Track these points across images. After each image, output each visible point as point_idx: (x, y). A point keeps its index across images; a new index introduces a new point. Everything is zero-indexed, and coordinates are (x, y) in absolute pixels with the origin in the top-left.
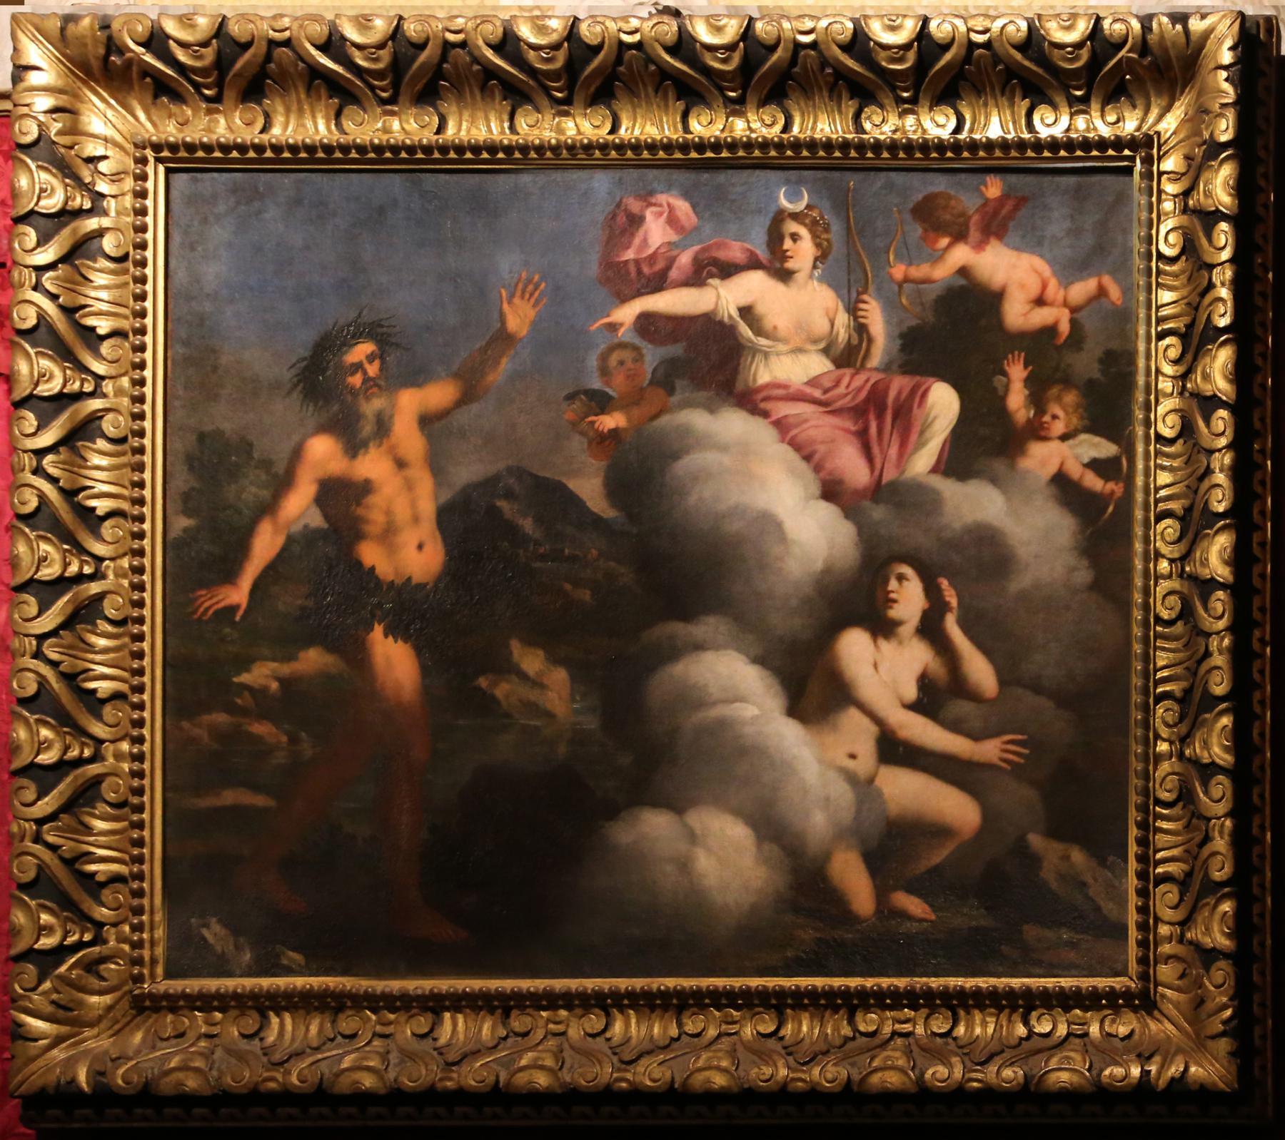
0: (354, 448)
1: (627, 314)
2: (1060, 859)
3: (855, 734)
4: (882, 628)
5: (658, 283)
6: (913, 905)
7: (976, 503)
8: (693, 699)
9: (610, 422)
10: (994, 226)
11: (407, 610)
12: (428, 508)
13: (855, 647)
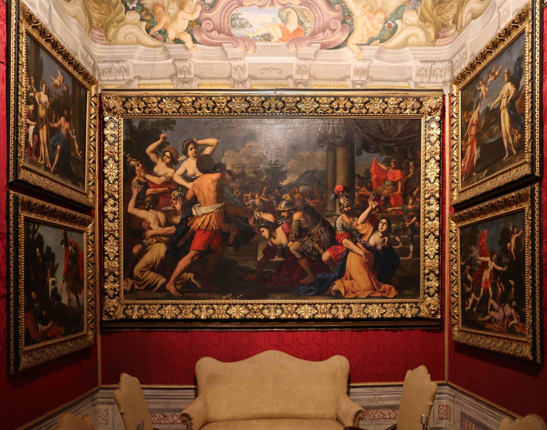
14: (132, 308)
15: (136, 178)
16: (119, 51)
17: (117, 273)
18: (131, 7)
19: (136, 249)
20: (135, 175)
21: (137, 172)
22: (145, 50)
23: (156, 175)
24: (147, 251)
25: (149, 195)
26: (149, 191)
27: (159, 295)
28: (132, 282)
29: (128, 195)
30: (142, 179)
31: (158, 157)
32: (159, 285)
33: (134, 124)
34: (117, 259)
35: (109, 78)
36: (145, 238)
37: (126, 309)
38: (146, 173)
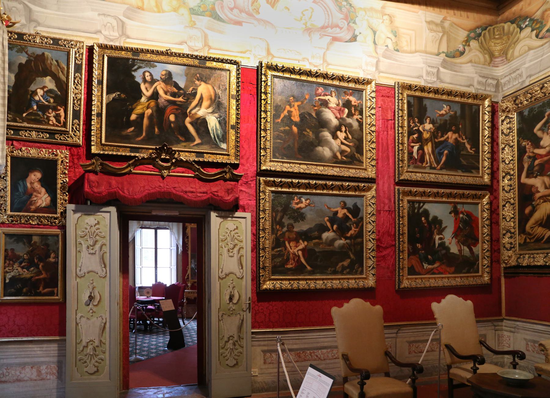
0: (291, 108)
1: (317, 98)
2: (357, 155)
3: (338, 141)
4: (341, 131)
5: (320, 96)
6: (344, 158)
7: (349, 120)
8: (324, 136)
9: (316, 108)
10: (351, 95)
11: (296, 124)
12: (298, 114)
13: (339, 133)
14: (524, 257)
15: (527, 154)
16: (514, 64)
17: (513, 230)
18: (524, 26)
19: (527, 211)
20: (526, 152)
21: (527, 150)
22: (535, 52)
23: (542, 147)
24: (536, 211)
25: (537, 165)
26: (537, 162)
27: (546, 246)
28: (525, 236)
29: (520, 169)
30: (531, 154)
31: (543, 133)
32: (546, 237)
33: (525, 114)
34: (512, 220)
35: (509, 87)
36: (534, 200)
37: (519, 258)
38: (534, 148)
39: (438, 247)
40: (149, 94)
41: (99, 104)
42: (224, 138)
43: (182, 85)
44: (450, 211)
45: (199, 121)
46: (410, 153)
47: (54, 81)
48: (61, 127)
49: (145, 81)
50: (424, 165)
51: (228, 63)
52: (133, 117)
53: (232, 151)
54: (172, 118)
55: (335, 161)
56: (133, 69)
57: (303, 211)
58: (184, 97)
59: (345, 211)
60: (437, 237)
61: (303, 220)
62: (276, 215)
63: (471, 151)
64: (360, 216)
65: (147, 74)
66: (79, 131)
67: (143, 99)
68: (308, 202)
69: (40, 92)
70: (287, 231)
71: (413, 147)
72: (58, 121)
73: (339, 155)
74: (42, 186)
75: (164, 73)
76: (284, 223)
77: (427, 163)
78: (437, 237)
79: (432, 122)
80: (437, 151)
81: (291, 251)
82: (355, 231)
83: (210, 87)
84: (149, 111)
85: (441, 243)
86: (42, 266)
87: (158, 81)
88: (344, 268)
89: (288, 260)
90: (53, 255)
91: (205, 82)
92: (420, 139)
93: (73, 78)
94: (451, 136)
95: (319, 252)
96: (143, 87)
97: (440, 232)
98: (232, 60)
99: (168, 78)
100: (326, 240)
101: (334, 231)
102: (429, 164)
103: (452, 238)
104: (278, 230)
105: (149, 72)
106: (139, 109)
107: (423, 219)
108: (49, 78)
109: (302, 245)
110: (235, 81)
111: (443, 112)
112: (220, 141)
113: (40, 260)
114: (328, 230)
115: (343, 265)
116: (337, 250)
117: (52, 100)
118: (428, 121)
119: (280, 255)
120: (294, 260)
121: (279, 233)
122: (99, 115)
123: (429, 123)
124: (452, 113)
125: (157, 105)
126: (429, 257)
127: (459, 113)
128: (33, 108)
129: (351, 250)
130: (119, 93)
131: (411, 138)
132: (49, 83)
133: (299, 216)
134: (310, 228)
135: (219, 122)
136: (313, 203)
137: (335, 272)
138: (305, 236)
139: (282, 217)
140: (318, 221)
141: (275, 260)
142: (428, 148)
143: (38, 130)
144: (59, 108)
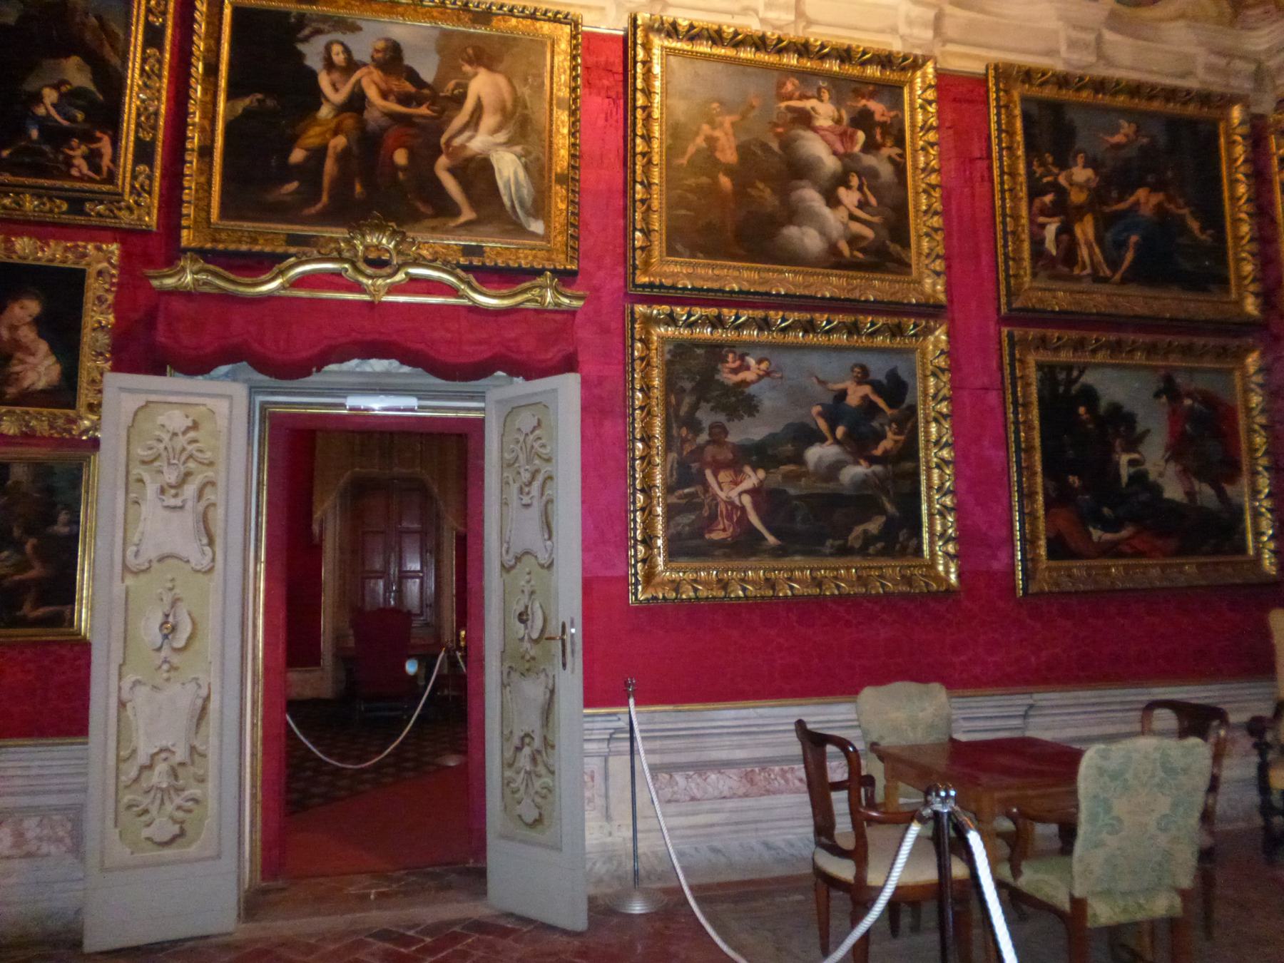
0: (714, 128)
1: (783, 105)
2: (895, 248)
3: (842, 213)
4: (849, 187)
5: (790, 98)
6: (860, 255)
7: (869, 160)
8: (802, 200)
9: (780, 130)
10: (872, 96)
11: (729, 171)
12: (733, 145)
13: (842, 192)
39: (1128, 485)
40: (338, 97)
41: (206, 123)
42: (540, 208)
43: (428, 75)
44: (1154, 389)
45: (473, 165)
46: (1037, 243)
47: (88, 68)
48: (104, 182)
49: (330, 65)
50: (1076, 271)
51: (549, 20)
52: (297, 155)
53: (559, 238)
54: (401, 157)
55: (833, 260)
56: (301, 35)
57: (752, 390)
58: (433, 104)
59: (866, 389)
60: (1124, 459)
61: (751, 415)
62: (679, 404)
63: (1203, 237)
64: (908, 401)
65: (336, 49)
66: (150, 193)
67: (325, 112)
68: (764, 366)
69: (50, 96)
70: (708, 443)
71: (1043, 226)
72: (96, 168)
73: (846, 250)
74: (41, 335)
75: (381, 45)
76: (700, 423)
77: (1084, 267)
78: (1124, 459)
79: (1091, 163)
80: (1109, 236)
81: (722, 495)
82: (896, 442)
83: (501, 80)
84: (339, 142)
85: (1135, 473)
86: (34, 547)
87: (365, 65)
88: (868, 540)
89: (713, 518)
90: (63, 517)
91: (490, 68)
92: (1062, 208)
93: (138, 60)
94: (1145, 199)
95: (798, 497)
96: (324, 81)
97: (1133, 443)
98: (558, 13)
99: (391, 59)
100: (818, 464)
101: (837, 442)
102: (1088, 271)
103: (1167, 461)
104: (684, 441)
105: (342, 44)
106: (312, 137)
107: (1082, 410)
108: (74, 61)
109: (752, 478)
110: (567, 64)
111: (1118, 138)
112: (528, 214)
113: (29, 531)
114: (822, 439)
115: (865, 532)
116: (846, 492)
117: (80, 116)
118: (1080, 159)
119: (691, 505)
120: (729, 517)
121: (688, 448)
122: (206, 152)
123: (1085, 167)
124: (1145, 140)
125: (362, 124)
126: (1106, 510)
127: (1162, 140)
128: (30, 137)
129: (887, 493)
130: (260, 96)
131: (1037, 203)
132: (76, 73)
133: (740, 403)
134: (773, 436)
135: (526, 167)
136: (779, 369)
137: (844, 551)
138: (760, 455)
139: (695, 407)
140: (795, 415)
141: (679, 519)
142: (1085, 230)
143: (38, 193)
144: (98, 134)
